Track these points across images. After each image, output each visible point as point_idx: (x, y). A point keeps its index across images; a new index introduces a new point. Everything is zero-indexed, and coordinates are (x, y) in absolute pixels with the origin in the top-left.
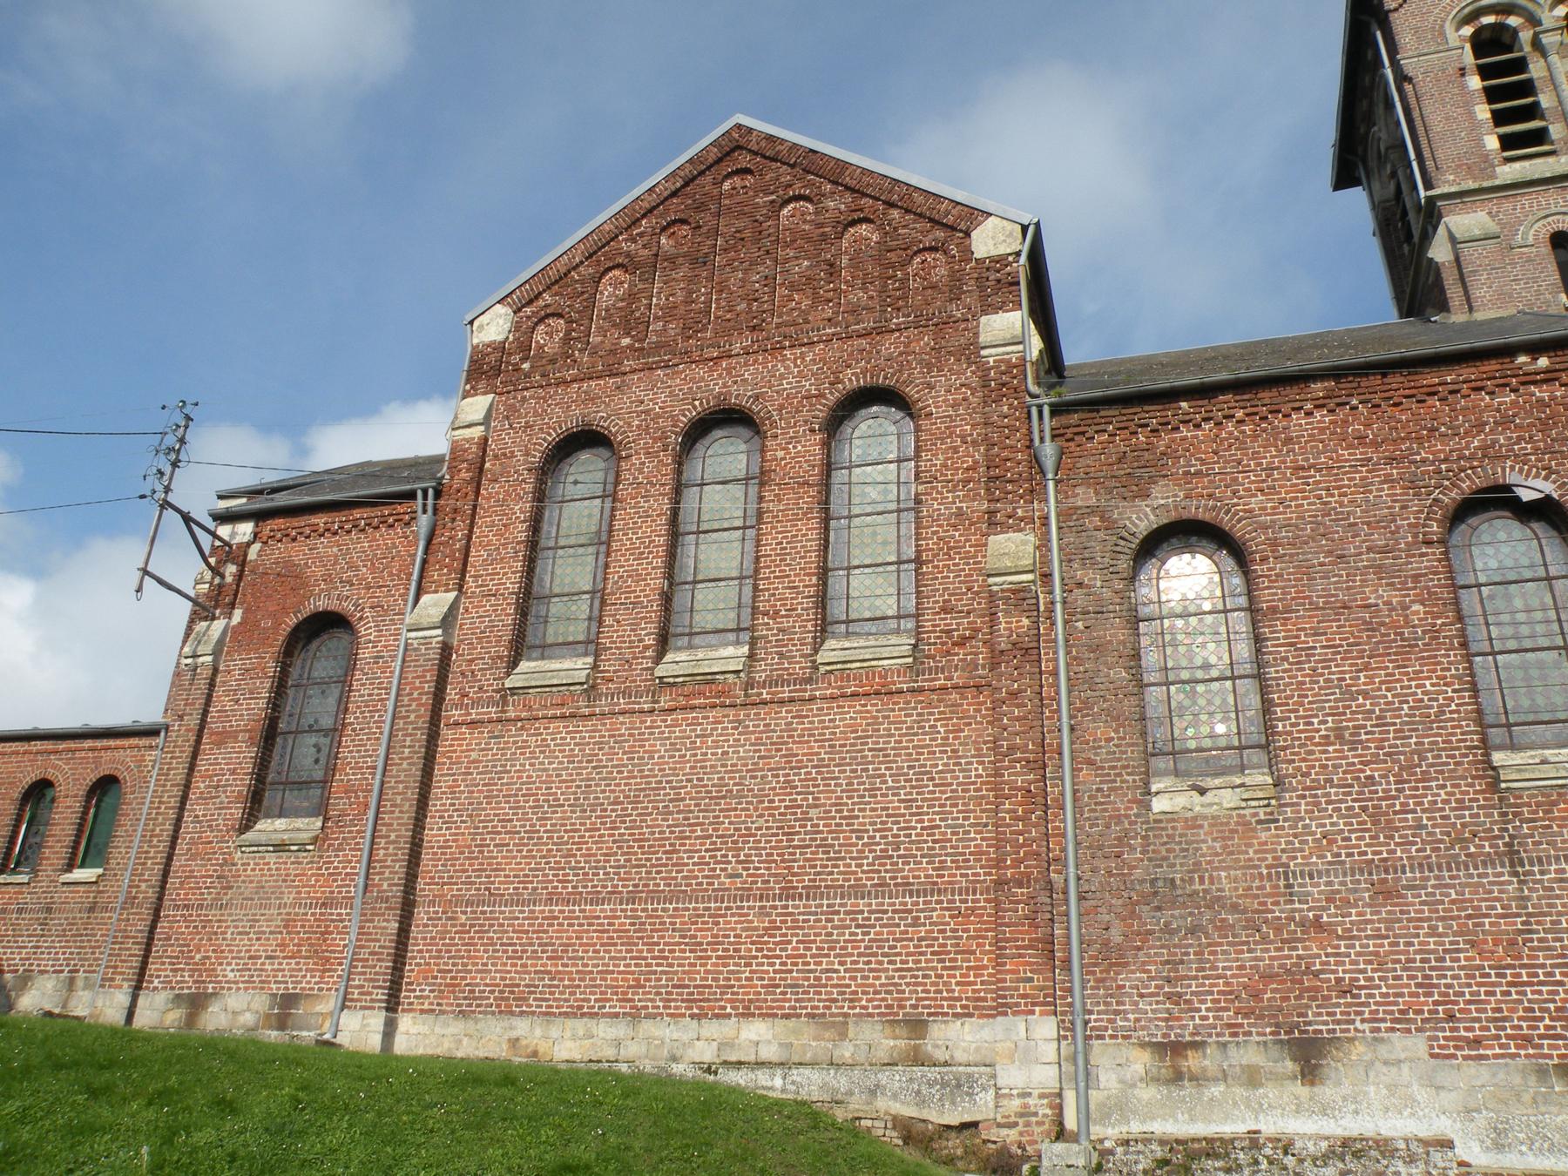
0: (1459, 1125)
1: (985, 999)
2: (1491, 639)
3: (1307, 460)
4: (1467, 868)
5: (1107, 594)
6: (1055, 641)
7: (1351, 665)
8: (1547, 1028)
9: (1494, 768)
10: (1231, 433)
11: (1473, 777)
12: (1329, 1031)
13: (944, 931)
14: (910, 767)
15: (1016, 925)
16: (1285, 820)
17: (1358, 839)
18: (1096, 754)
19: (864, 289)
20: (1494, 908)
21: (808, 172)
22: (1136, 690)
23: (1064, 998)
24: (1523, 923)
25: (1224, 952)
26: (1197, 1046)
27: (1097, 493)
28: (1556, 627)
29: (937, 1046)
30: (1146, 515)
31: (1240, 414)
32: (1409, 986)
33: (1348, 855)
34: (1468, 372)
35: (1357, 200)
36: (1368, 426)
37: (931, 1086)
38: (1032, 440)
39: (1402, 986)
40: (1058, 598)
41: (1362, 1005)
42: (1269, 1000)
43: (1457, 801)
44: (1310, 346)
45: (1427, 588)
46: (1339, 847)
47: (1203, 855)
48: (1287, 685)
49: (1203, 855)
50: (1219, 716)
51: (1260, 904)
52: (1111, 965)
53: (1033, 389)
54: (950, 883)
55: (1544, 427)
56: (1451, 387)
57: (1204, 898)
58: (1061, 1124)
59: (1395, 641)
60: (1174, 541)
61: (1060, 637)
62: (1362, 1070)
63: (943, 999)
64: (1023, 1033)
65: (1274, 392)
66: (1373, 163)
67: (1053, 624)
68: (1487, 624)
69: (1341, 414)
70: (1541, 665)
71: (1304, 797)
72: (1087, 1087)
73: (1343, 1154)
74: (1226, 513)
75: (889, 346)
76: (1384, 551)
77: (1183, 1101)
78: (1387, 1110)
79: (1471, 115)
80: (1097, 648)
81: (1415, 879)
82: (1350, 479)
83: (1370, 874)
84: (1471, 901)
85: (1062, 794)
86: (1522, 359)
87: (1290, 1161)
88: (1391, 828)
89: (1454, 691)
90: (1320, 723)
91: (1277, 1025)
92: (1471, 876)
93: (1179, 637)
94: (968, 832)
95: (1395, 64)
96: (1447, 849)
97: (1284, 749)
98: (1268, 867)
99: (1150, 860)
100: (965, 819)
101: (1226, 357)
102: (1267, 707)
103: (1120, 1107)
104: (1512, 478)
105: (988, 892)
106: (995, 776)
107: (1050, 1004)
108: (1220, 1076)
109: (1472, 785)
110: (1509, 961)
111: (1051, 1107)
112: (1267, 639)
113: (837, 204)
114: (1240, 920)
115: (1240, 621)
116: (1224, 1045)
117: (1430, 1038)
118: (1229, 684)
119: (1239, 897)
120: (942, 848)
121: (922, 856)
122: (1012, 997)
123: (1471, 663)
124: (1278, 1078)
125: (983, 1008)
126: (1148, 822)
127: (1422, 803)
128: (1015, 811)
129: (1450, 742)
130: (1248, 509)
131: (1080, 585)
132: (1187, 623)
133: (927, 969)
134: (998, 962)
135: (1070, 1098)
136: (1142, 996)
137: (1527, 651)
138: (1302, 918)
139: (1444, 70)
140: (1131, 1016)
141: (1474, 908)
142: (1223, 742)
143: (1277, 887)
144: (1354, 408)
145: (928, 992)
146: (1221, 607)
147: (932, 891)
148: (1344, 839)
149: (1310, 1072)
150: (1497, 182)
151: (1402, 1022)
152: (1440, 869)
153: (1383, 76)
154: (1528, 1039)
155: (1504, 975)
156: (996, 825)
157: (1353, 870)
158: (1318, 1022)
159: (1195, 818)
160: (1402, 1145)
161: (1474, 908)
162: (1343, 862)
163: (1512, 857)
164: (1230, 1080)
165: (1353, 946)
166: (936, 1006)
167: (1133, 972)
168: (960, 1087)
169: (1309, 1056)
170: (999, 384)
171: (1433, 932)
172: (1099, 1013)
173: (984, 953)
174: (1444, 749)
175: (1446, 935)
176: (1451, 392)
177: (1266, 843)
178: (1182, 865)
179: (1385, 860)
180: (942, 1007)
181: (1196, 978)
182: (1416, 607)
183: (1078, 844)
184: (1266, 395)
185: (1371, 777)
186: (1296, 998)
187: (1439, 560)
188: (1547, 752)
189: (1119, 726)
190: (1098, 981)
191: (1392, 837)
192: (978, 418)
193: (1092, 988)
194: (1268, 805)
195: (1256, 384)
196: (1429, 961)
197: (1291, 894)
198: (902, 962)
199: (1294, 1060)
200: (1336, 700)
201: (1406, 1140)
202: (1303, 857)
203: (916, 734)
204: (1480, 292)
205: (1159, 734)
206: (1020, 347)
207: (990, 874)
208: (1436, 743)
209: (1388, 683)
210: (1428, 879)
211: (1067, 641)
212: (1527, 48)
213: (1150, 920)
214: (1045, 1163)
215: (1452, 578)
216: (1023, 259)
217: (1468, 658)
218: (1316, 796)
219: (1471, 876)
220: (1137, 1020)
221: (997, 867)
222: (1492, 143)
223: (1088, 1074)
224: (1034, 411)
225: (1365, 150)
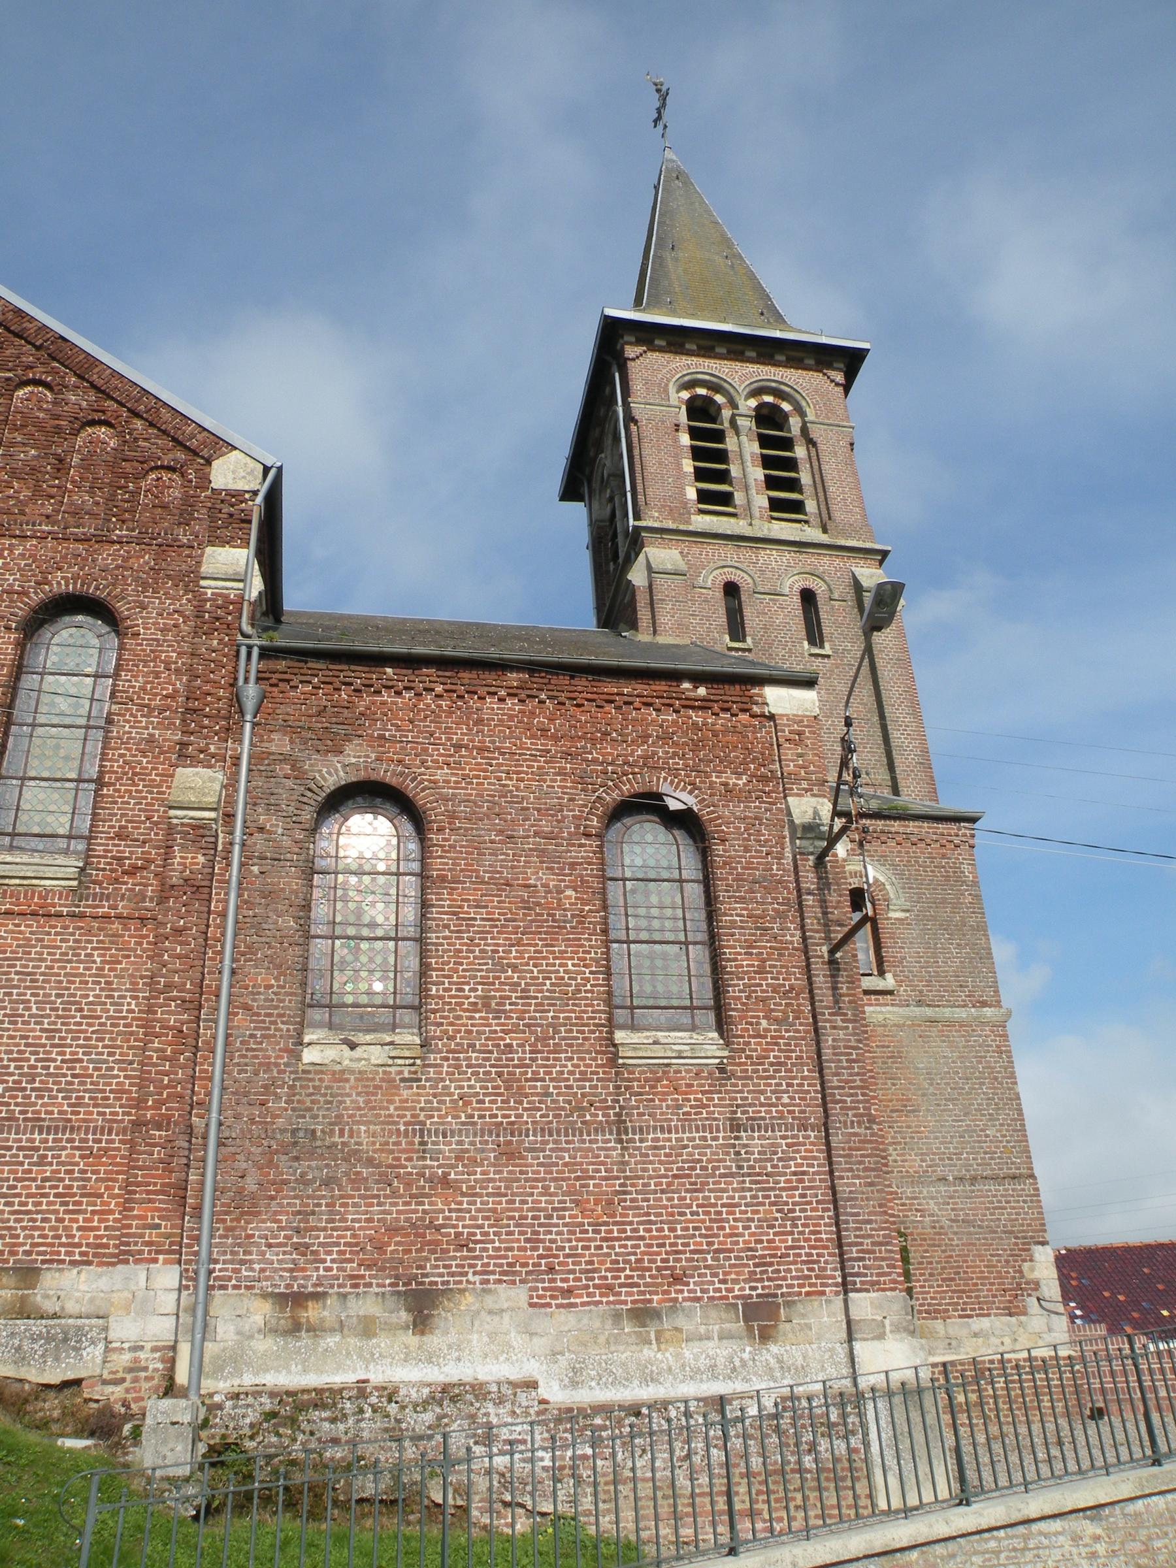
0: (544, 1367)
1: (106, 1246)
2: (627, 929)
3: (493, 742)
4: (581, 1135)
5: (286, 842)
6: (228, 882)
7: (506, 939)
8: (627, 1277)
9: (615, 1045)
10: (428, 705)
11: (597, 1052)
12: (443, 1283)
13: (71, 1172)
14: (58, 996)
15: (149, 1168)
16: (427, 1080)
17: (491, 1102)
18: (254, 1000)
19: (91, 492)
20: (599, 1171)
21: (54, 359)
22: (301, 941)
23: (191, 1246)
24: (621, 1185)
25: (355, 1205)
26: (317, 1296)
27: (292, 742)
28: (681, 923)
29: (47, 1297)
30: (336, 770)
31: (439, 689)
32: (518, 1241)
33: (480, 1117)
34: (641, 688)
35: (578, 511)
36: (551, 720)
37: (34, 1341)
38: (236, 679)
39: (513, 1241)
40: (238, 840)
41: (475, 1258)
42: (392, 1252)
43: (581, 1073)
44: (514, 637)
45: (581, 876)
46: (474, 1109)
47: (346, 1109)
48: (444, 951)
49: (346, 1109)
50: (378, 975)
51: (394, 1159)
52: (243, 1213)
53: (246, 628)
54: (84, 1120)
55: (696, 747)
56: (626, 699)
57: (342, 1151)
58: (171, 1379)
59: (547, 921)
60: (359, 799)
61: (234, 879)
62: (468, 1319)
63: (61, 1245)
64: (143, 1283)
65: (474, 674)
66: (596, 485)
67: (229, 865)
68: (627, 915)
69: (531, 705)
70: (665, 957)
71: (447, 1059)
72: (204, 1339)
73: (442, 1399)
74: (413, 780)
75: (107, 557)
76: (549, 837)
77: (298, 1352)
78: (486, 1356)
79: (679, 466)
80: (269, 895)
81: (536, 1142)
82: (528, 767)
83: (498, 1136)
84: (581, 1164)
85: (215, 1037)
86: (686, 685)
87: (393, 1408)
88: (521, 1094)
89: (591, 973)
90: (471, 990)
91: (397, 1277)
92: (584, 1141)
93: (351, 893)
94: (112, 1069)
95: (626, 404)
96: (567, 1116)
97: (434, 1011)
98: (406, 1124)
99: (293, 1109)
100: (110, 1054)
101: (438, 632)
102: (424, 970)
103: (235, 1360)
104: (664, 788)
105: (125, 1134)
106: (148, 1012)
107: (175, 1252)
108: (337, 1326)
109: (595, 1059)
110: (605, 1219)
111: (163, 1361)
112: (433, 906)
113: (78, 399)
114: (373, 1174)
115: (410, 885)
116: (344, 1296)
117: (531, 1289)
118: (391, 944)
119: (375, 1151)
120: (81, 1083)
121: (59, 1091)
122: (136, 1244)
123: (608, 948)
124: (392, 1329)
125: (104, 1255)
126: (296, 1072)
127: (550, 1073)
128: (164, 1051)
129: (582, 1018)
130: (433, 778)
131: (261, 829)
132: (360, 881)
133: (48, 1212)
134: (126, 1208)
135: (184, 1349)
136: (270, 1246)
137: (655, 942)
138: (431, 1174)
139: (663, 422)
140: (257, 1266)
141: (582, 1171)
142: (378, 1000)
143: (412, 1143)
144: (542, 702)
145: (45, 1237)
146: (394, 870)
147: (64, 1129)
148: (479, 1102)
149: (421, 1322)
150: (691, 528)
151: (509, 1275)
152: (559, 1134)
153: (616, 412)
154: (610, 1288)
155: (599, 1232)
156: (142, 1063)
157: (482, 1130)
158: (435, 1274)
159: (343, 1072)
160: (494, 1388)
161: (582, 1171)
162: (475, 1124)
163: (620, 1125)
164: (346, 1331)
165: (475, 1203)
166: (52, 1253)
167: (264, 1221)
168: (66, 1342)
169: (422, 1306)
170: (213, 617)
171: (546, 1192)
172: (225, 1262)
173: (111, 1196)
174: (576, 1025)
175: (556, 1195)
176: (626, 703)
177: (406, 1101)
178: (324, 1117)
179: (512, 1123)
180: (59, 1253)
181: (325, 1229)
182: (569, 892)
183: (223, 1089)
184: (466, 675)
185: (510, 1046)
186: (417, 1251)
187: (595, 852)
188: (660, 1034)
189: (280, 974)
190: (227, 1229)
191: (521, 1103)
192: (186, 647)
193: (221, 1237)
194: (413, 1065)
195: (458, 663)
196: (538, 1218)
197: (424, 1151)
198: (21, 1204)
199: (409, 1310)
200: (488, 971)
201: (499, 1384)
202: (439, 1117)
203: (70, 961)
204: (664, 619)
205: (318, 986)
206: (241, 585)
207: (129, 1114)
208: (569, 1018)
209: (536, 959)
210: (547, 1142)
211: (240, 883)
212: (726, 424)
213: (286, 1168)
214: (149, 1421)
215: (603, 870)
216: (259, 499)
217: (607, 943)
218: (458, 1059)
219: (584, 1141)
220: (262, 1270)
221: (138, 1107)
222: (691, 494)
223: (205, 1325)
224: (243, 650)
225: (592, 472)
